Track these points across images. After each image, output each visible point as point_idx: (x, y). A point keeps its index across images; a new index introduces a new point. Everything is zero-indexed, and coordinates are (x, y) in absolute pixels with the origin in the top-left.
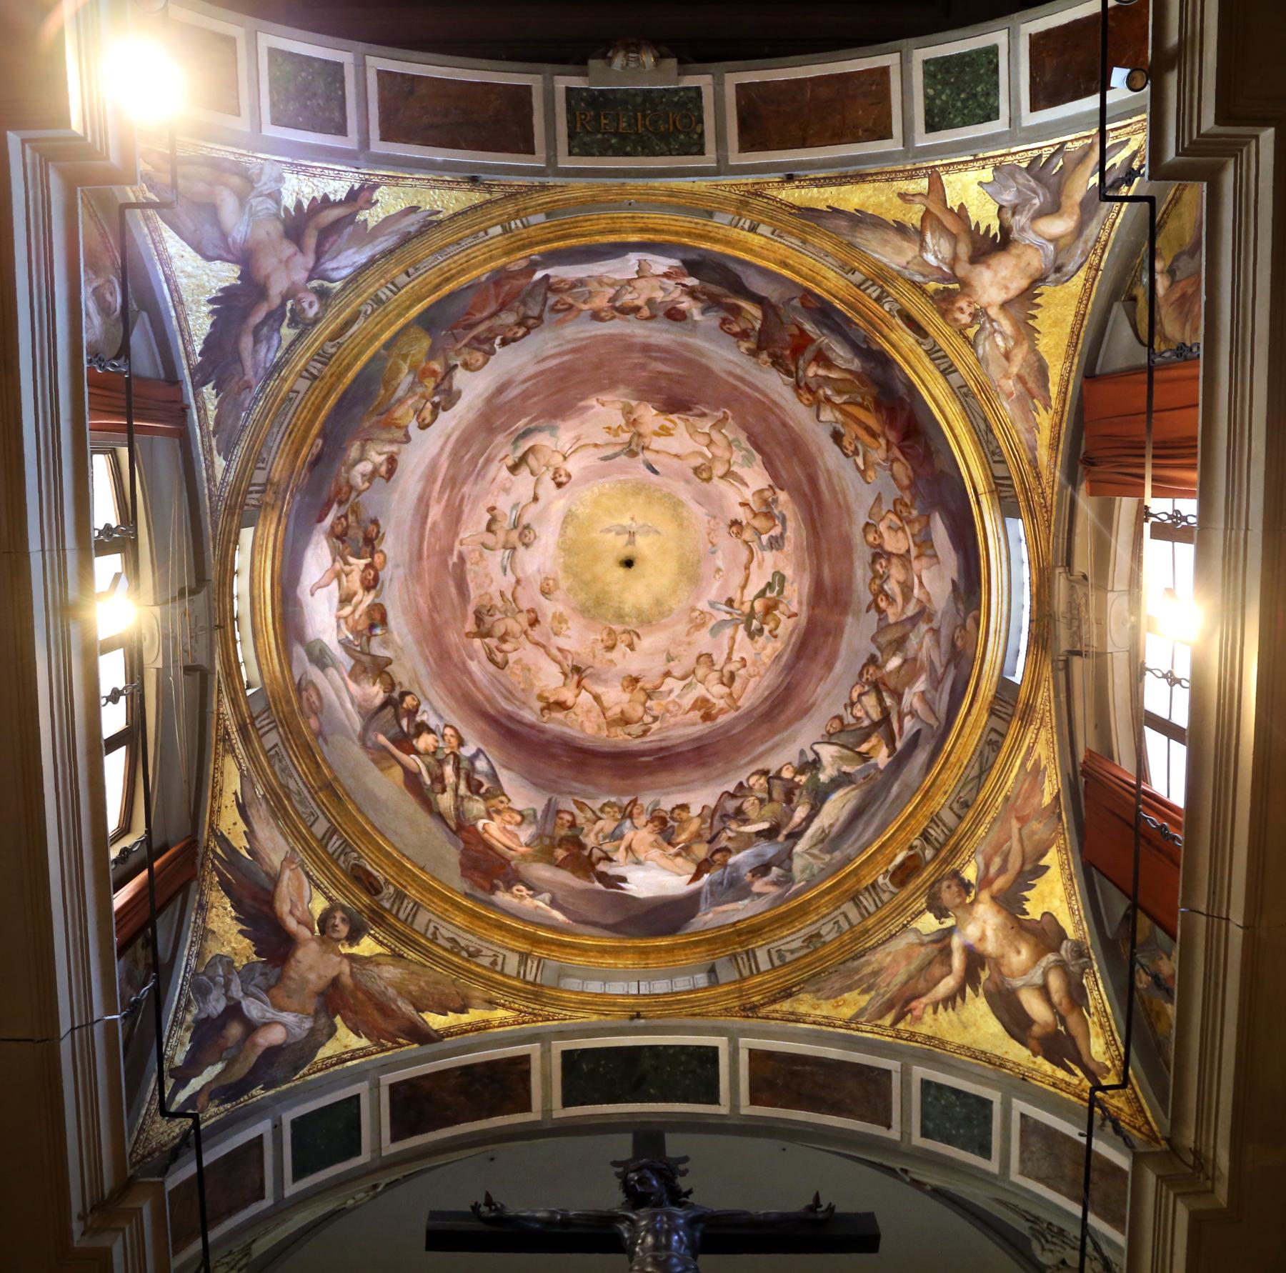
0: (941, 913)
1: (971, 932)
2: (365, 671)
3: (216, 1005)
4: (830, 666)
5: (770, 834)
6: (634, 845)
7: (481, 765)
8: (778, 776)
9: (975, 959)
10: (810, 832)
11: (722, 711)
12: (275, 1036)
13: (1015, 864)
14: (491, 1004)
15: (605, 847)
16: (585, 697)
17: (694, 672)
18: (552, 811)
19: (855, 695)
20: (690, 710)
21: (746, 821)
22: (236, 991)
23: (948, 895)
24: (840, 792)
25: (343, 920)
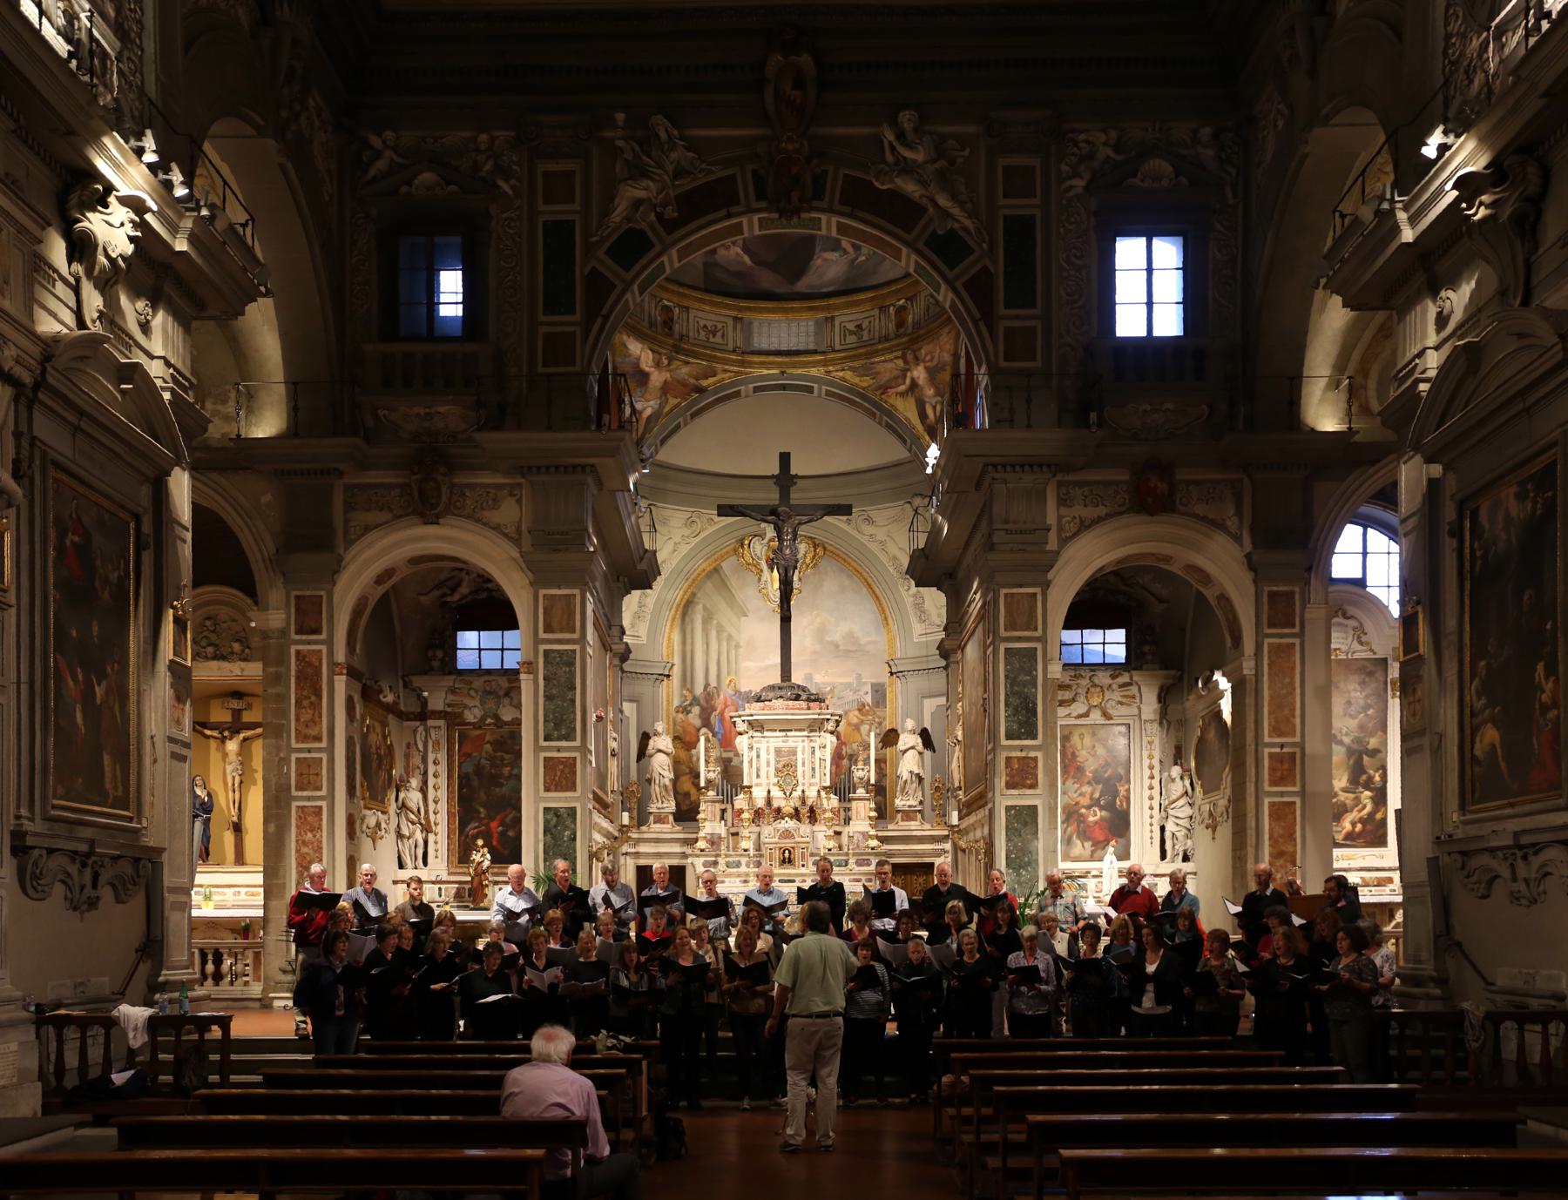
0: (906, 362)
1: (915, 374)
9: (914, 385)
12: (648, 412)
14: (725, 371)
23: (910, 357)
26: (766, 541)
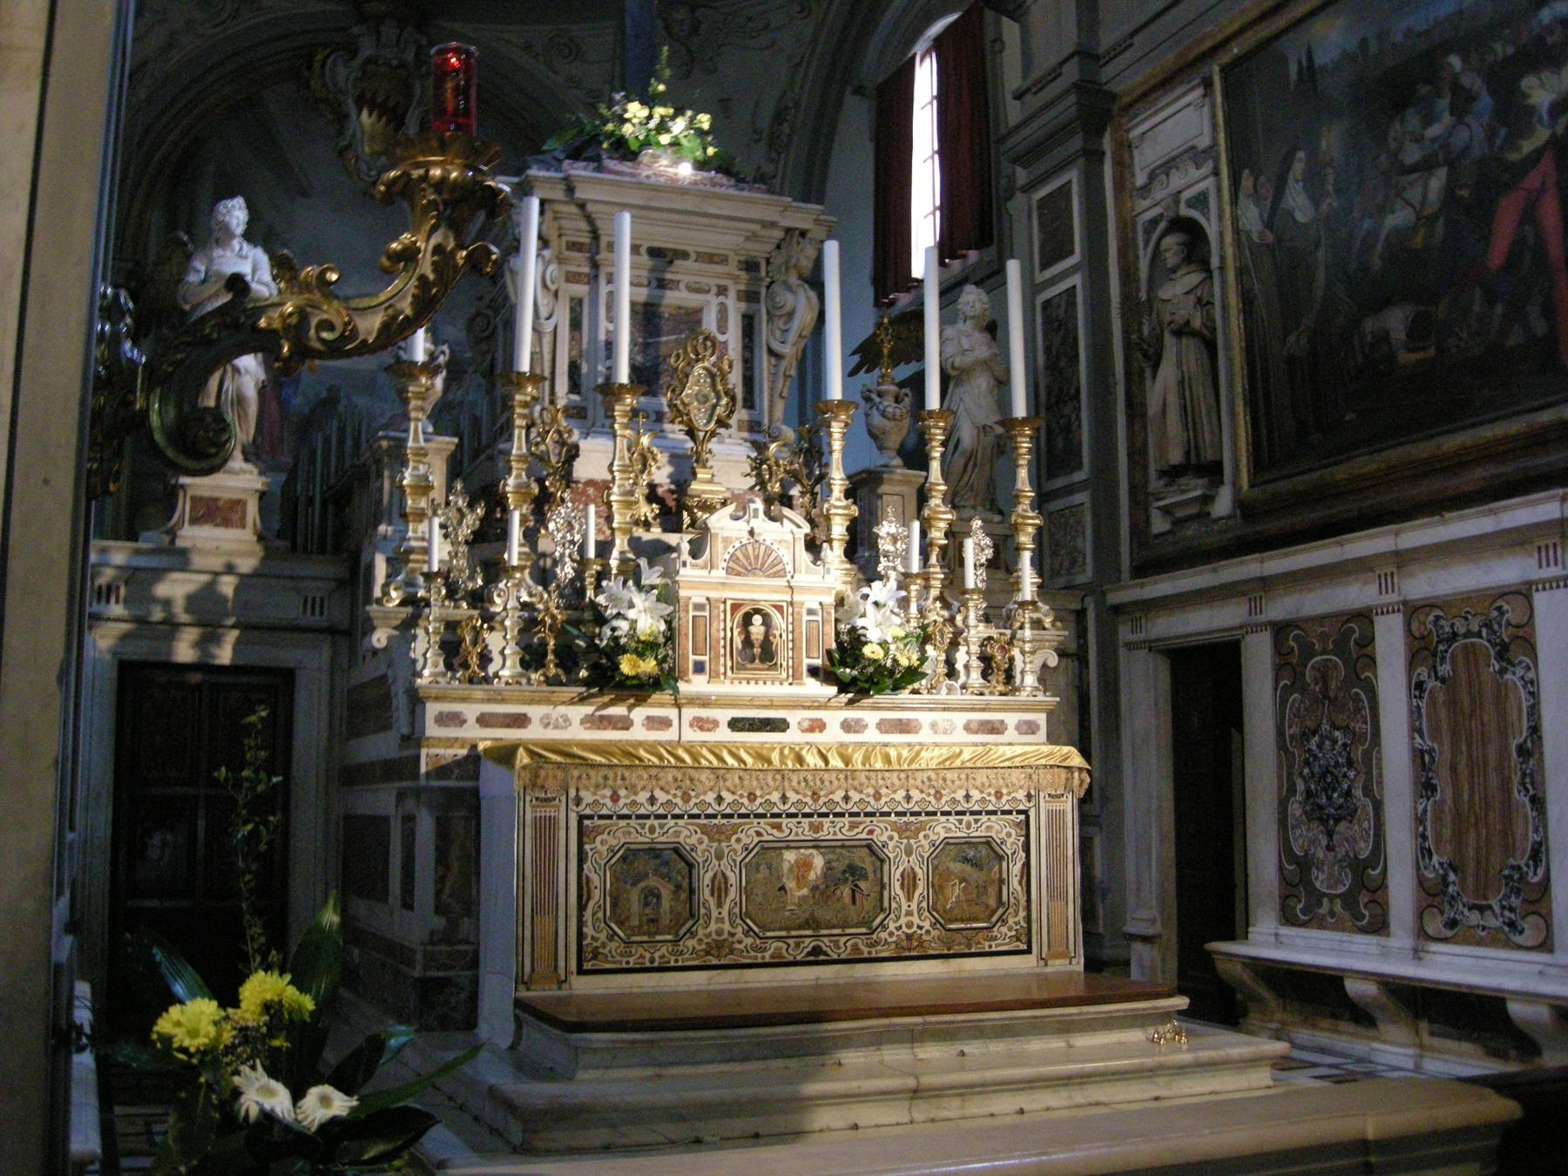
26: (359, 61)
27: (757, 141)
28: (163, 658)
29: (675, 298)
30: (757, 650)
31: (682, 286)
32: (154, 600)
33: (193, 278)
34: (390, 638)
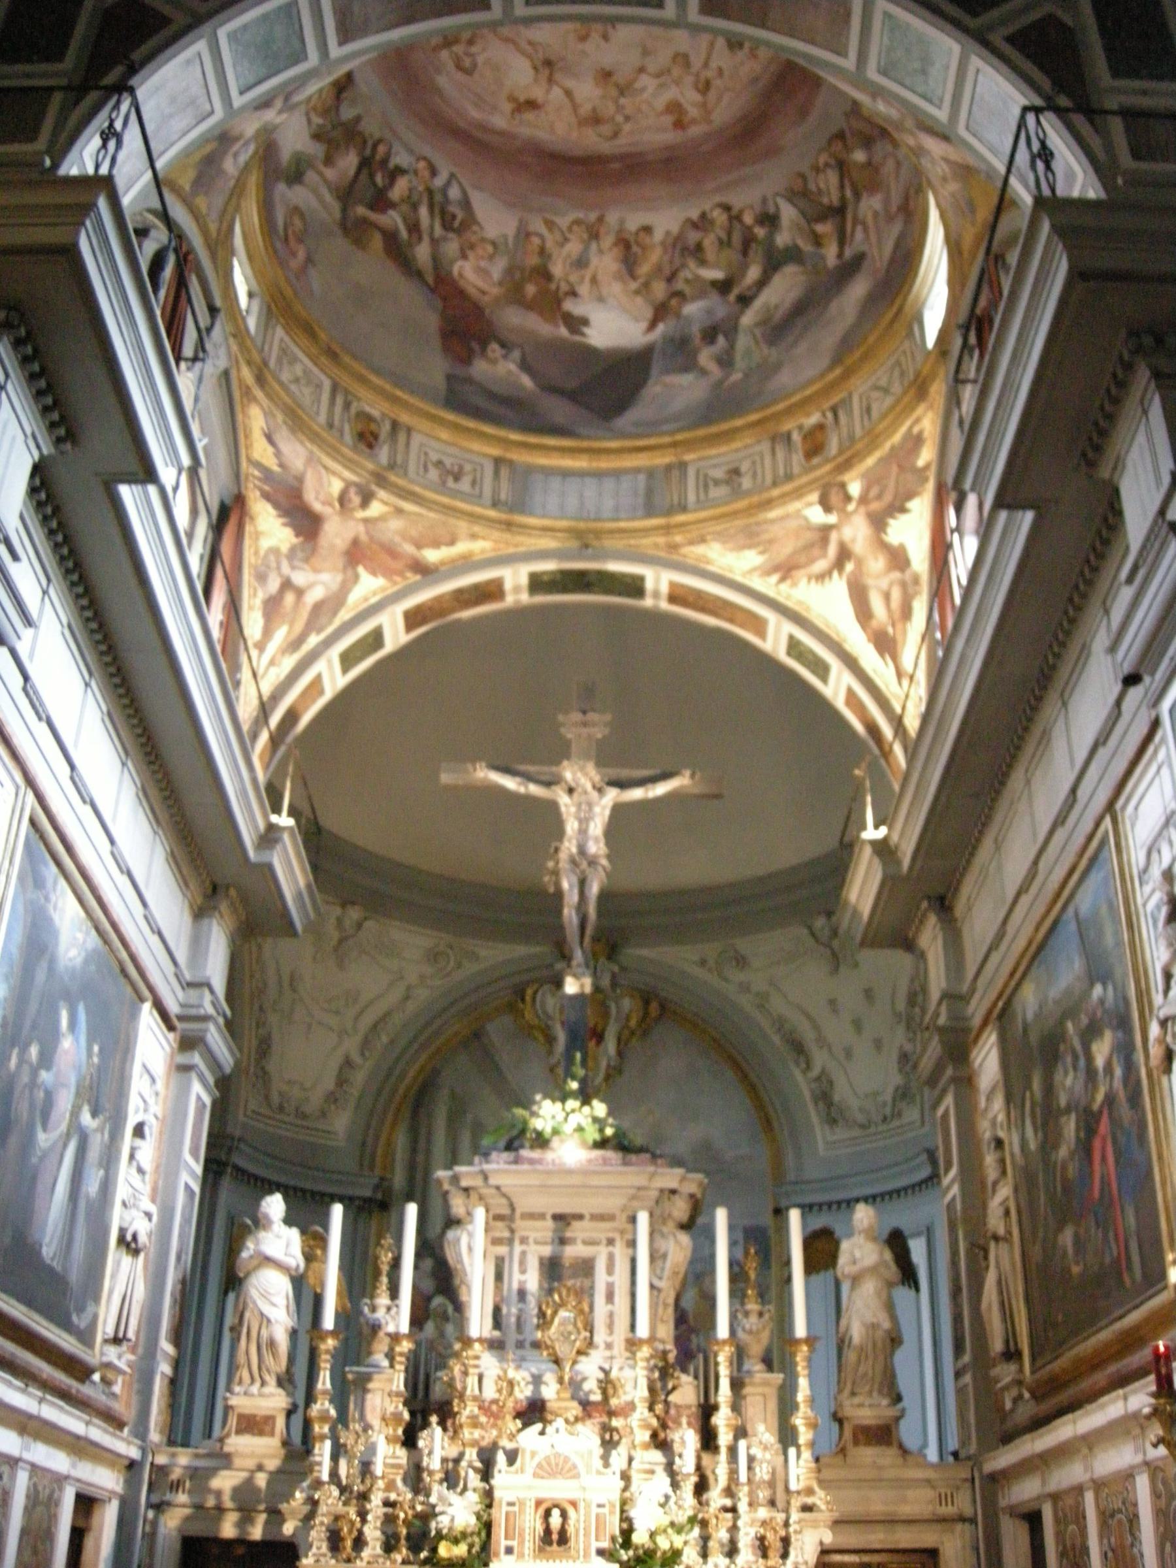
0: (827, 508)
1: (847, 533)
2: (338, 147)
3: (274, 585)
4: (804, 113)
5: (724, 287)
6: (599, 277)
7: (454, 193)
8: (738, 218)
9: (844, 554)
10: (758, 304)
11: (694, 121)
13: (888, 498)
14: (474, 537)
15: (573, 278)
16: (557, 92)
17: (669, 71)
18: (524, 234)
19: (822, 159)
20: (662, 114)
21: (703, 262)
22: (286, 569)
23: (835, 498)
24: (790, 270)
25: (357, 493)
27: (899, 1022)
28: (211, 1535)
29: (571, 1252)
30: (555, 1537)
31: (579, 1241)
32: (209, 1491)
33: (245, 1254)
34: (296, 1529)
